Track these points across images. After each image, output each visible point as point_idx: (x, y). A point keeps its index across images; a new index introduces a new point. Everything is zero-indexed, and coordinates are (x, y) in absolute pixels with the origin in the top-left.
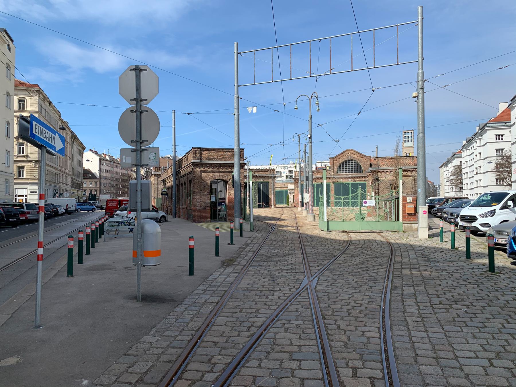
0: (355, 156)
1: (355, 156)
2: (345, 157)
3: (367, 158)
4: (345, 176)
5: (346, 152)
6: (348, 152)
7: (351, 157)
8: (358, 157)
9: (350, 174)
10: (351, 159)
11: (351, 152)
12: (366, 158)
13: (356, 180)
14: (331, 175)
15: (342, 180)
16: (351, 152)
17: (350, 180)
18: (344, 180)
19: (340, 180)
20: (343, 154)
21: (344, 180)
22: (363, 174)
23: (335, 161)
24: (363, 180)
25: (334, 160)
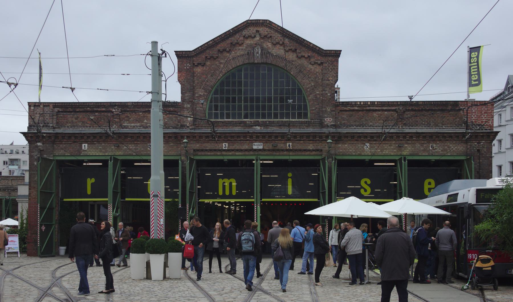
0: (278, 51)
1: (278, 51)
2: (239, 51)
3: (324, 60)
4: (237, 129)
5: (245, 32)
6: (252, 30)
7: (265, 52)
8: (291, 56)
9: (257, 124)
10: (264, 60)
11: (264, 30)
12: (320, 59)
13: (281, 146)
14: (183, 126)
15: (225, 146)
16: (264, 30)
17: (257, 146)
18: (237, 146)
19: (217, 146)
20: (233, 39)
21: (237, 146)
22: (308, 124)
23: (199, 70)
24: (311, 147)
25: (196, 60)
